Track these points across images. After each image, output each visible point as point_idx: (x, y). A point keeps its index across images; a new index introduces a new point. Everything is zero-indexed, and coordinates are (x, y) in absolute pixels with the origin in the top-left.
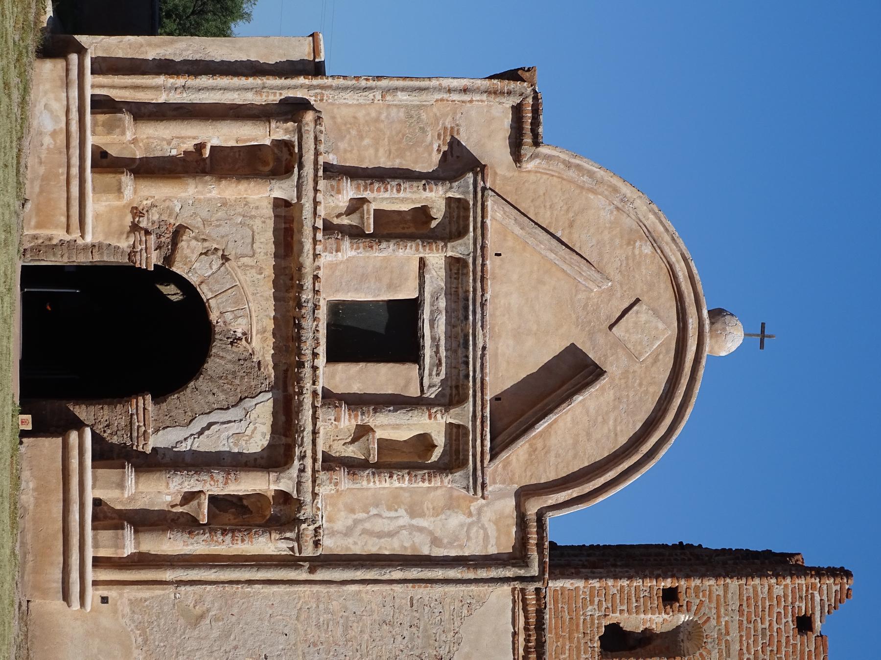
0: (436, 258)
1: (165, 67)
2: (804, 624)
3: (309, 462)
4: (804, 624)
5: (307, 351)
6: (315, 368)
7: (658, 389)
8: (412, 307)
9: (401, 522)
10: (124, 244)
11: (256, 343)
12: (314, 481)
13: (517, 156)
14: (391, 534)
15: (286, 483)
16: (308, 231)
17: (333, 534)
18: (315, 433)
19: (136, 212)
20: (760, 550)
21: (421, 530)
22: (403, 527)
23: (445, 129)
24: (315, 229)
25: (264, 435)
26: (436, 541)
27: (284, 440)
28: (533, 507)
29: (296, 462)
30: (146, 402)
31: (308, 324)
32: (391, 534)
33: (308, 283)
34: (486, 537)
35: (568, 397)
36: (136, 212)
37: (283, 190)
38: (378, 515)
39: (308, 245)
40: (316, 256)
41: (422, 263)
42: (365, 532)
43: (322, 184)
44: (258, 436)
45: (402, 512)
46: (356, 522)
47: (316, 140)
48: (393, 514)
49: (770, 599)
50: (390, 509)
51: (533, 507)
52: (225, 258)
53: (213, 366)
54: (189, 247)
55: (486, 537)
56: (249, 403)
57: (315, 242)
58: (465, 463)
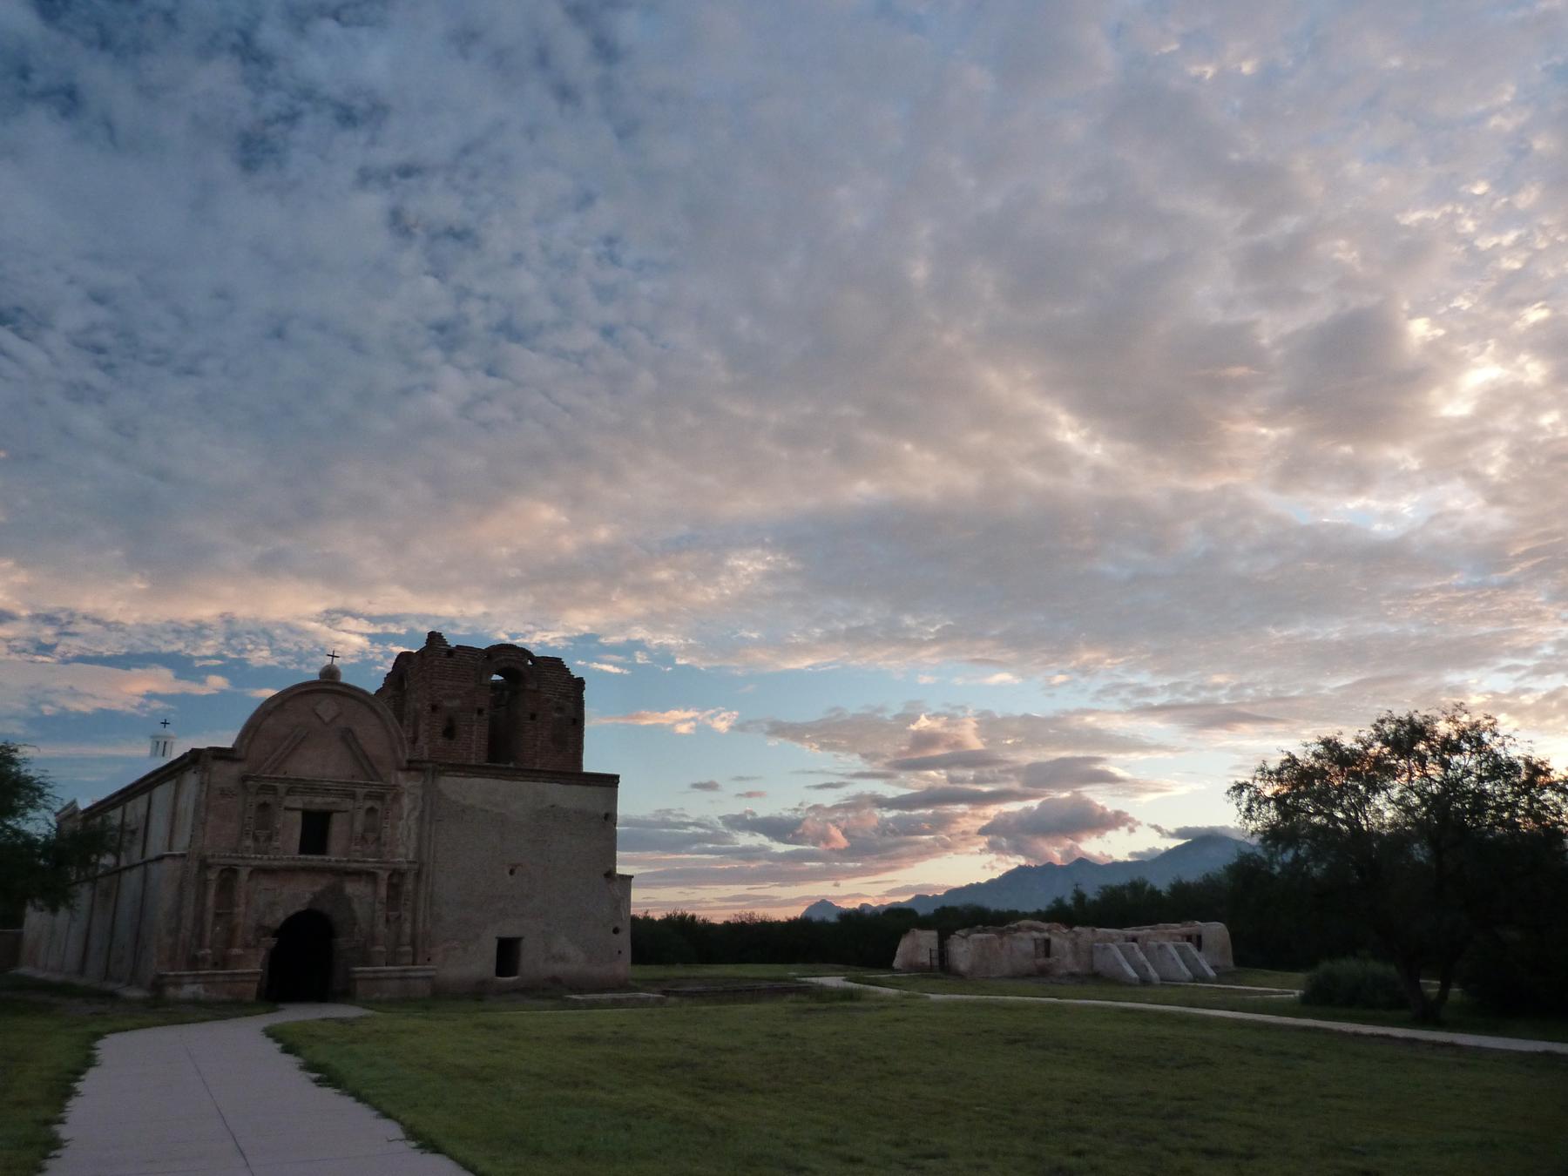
2: (451, 652)
3: (378, 865)
5: (327, 864)
6: (337, 861)
10: (263, 953)
11: (318, 888)
12: (387, 863)
13: (239, 760)
15: (384, 875)
16: (267, 863)
17: (406, 856)
18: (364, 862)
21: (408, 816)
24: (269, 859)
26: (414, 808)
29: (377, 871)
30: (341, 942)
31: (314, 864)
33: (292, 863)
37: (244, 874)
39: (276, 863)
40: (282, 859)
41: (287, 809)
43: (246, 855)
47: (225, 857)
57: (275, 859)
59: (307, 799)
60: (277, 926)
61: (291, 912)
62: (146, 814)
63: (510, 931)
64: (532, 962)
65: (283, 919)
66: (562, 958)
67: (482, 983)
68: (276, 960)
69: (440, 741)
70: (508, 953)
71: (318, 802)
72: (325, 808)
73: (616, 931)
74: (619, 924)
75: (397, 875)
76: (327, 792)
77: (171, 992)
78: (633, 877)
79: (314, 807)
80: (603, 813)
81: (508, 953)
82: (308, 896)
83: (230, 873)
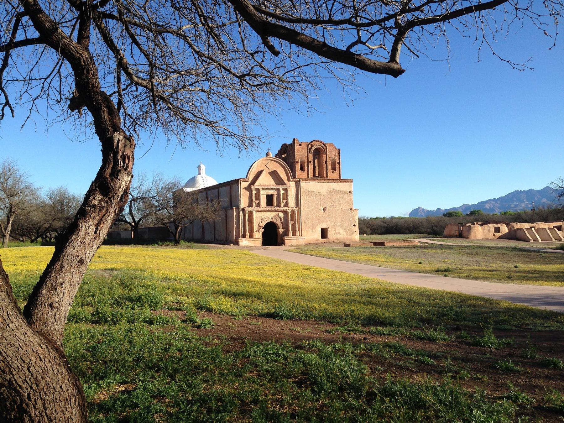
0: (262, 192)
1: (238, 227)
4: (300, 145)
7: (277, 164)
8: (267, 195)
15: (290, 211)
19: (256, 231)
20: (280, 149)
28: (291, 180)
35: (279, 176)
36: (256, 231)
37: (254, 212)
51: (291, 180)
52: (262, 220)
53: (275, 221)
54: (261, 225)
58: (287, 189)
59: (267, 191)
61: (266, 222)
63: (324, 226)
64: (331, 234)
66: (339, 233)
67: (318, 240)
68: (264, 235)
69: (300, 172)
70: (324, 233)
72: (272, 193)
73: (354, 225)
74: (355, 224)
75: (293, 212)
76: (272, 189)
77: (241, 244)
79: (268, 194)
80: (349, 191)
81: (324, 233)
82: (271, 218)
83: (251, 213)
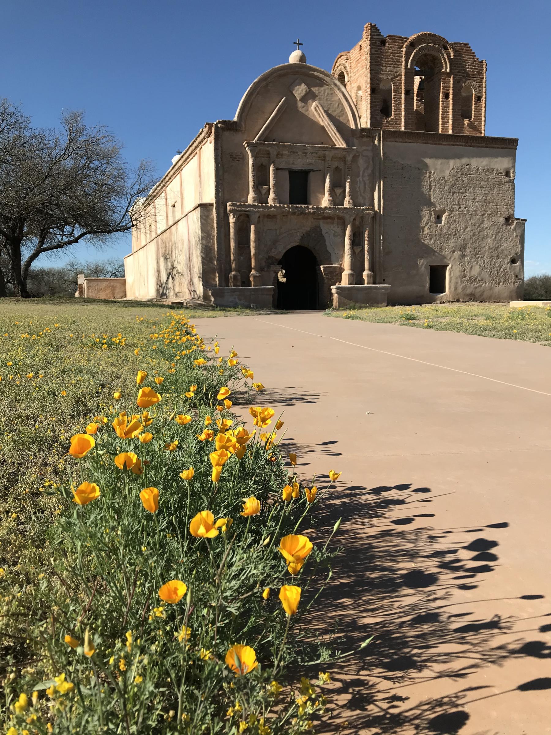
9: (361, 180)
14: (365, 184)
22: (363, 180)
23: (231, 158)
25: (334, 227)
27: (336, 220)
32: (365, 184)
34: (366, 150)
38: (359, 187)
42: (364, 193)
44: (334, 229)
45: (358, 179)
46: (361, 195)
48: (359, 183)
49: (376, 54)
50: (357, 184)
55: (366, 150)
56: (324, 232)
60: (280, 257)
61: (289, 247)
62: (179, 190)
65: (284, 251)
71: (299, 164)
78: (526, 220)
